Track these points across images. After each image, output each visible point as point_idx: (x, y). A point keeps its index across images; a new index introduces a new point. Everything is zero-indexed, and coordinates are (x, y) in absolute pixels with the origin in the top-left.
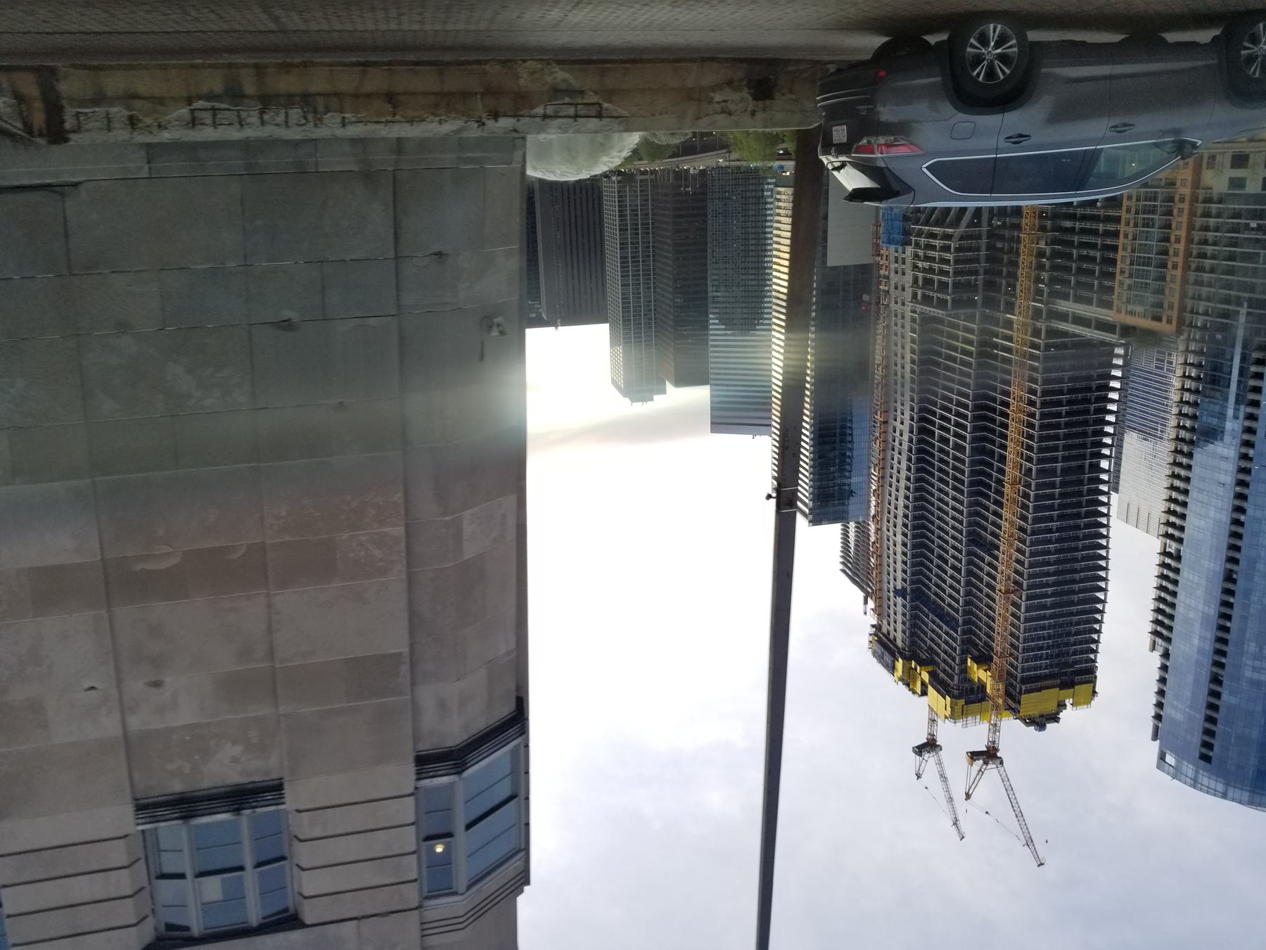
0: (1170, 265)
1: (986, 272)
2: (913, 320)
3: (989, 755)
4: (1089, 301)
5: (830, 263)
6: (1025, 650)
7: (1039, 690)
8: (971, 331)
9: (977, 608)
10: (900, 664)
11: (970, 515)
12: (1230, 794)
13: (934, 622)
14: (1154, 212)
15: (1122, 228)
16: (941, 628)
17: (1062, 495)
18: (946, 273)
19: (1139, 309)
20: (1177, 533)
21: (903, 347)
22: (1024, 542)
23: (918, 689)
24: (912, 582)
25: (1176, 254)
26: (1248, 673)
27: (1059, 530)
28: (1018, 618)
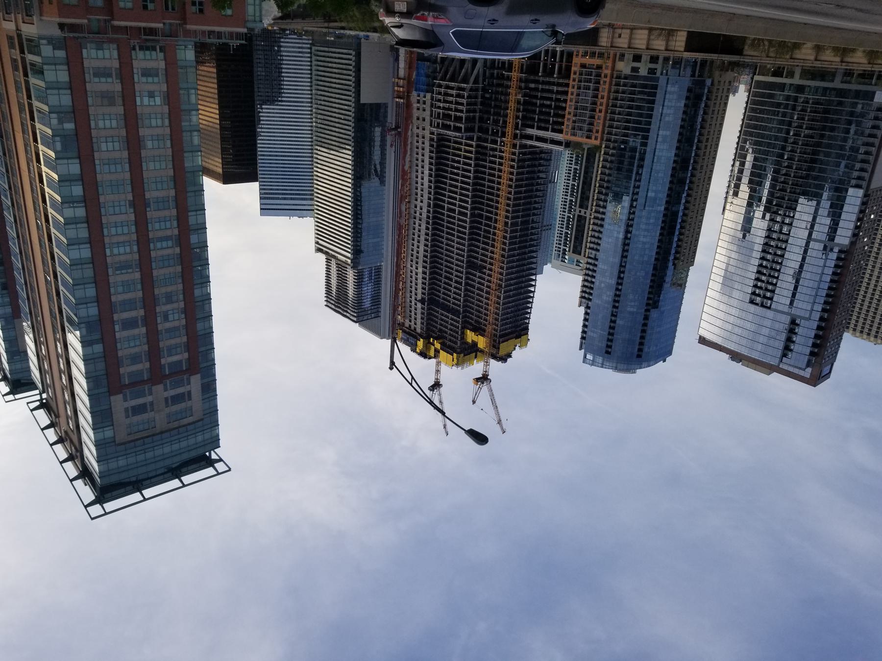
0: (597, 110)
1: (481, 111)
2: (432, 140)
3: (484, 379)
4: (547, 129)
5: (362, 101)
6: (502, 320)
7: (507, 340)
8: (471, 146)
9: (471, 302)
10: (420, 344)
11: (469, 251)
12: (619, 367)
13: (442, 315)
14: (590, 82)
15: (570, 90)
16: (448, 317)
17: (521, 236)
18: (462, 111)
19: (579, 132)
20: (595, 246)
21: (423, 155)
22: (503, 263)
23: (432, 353)
24: (429, 294)
25: (601, 104)
26: (629, 309)
27: (518, 255)
28: (499, 304)
